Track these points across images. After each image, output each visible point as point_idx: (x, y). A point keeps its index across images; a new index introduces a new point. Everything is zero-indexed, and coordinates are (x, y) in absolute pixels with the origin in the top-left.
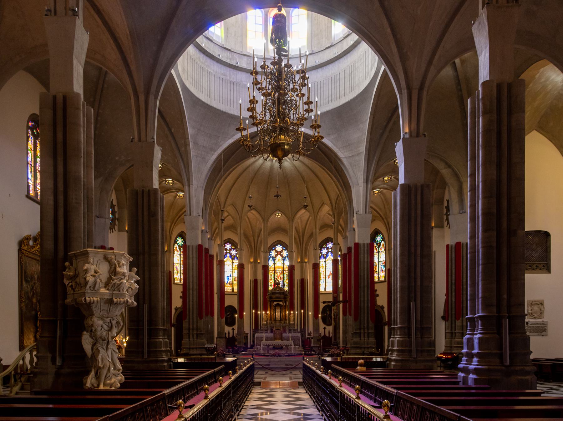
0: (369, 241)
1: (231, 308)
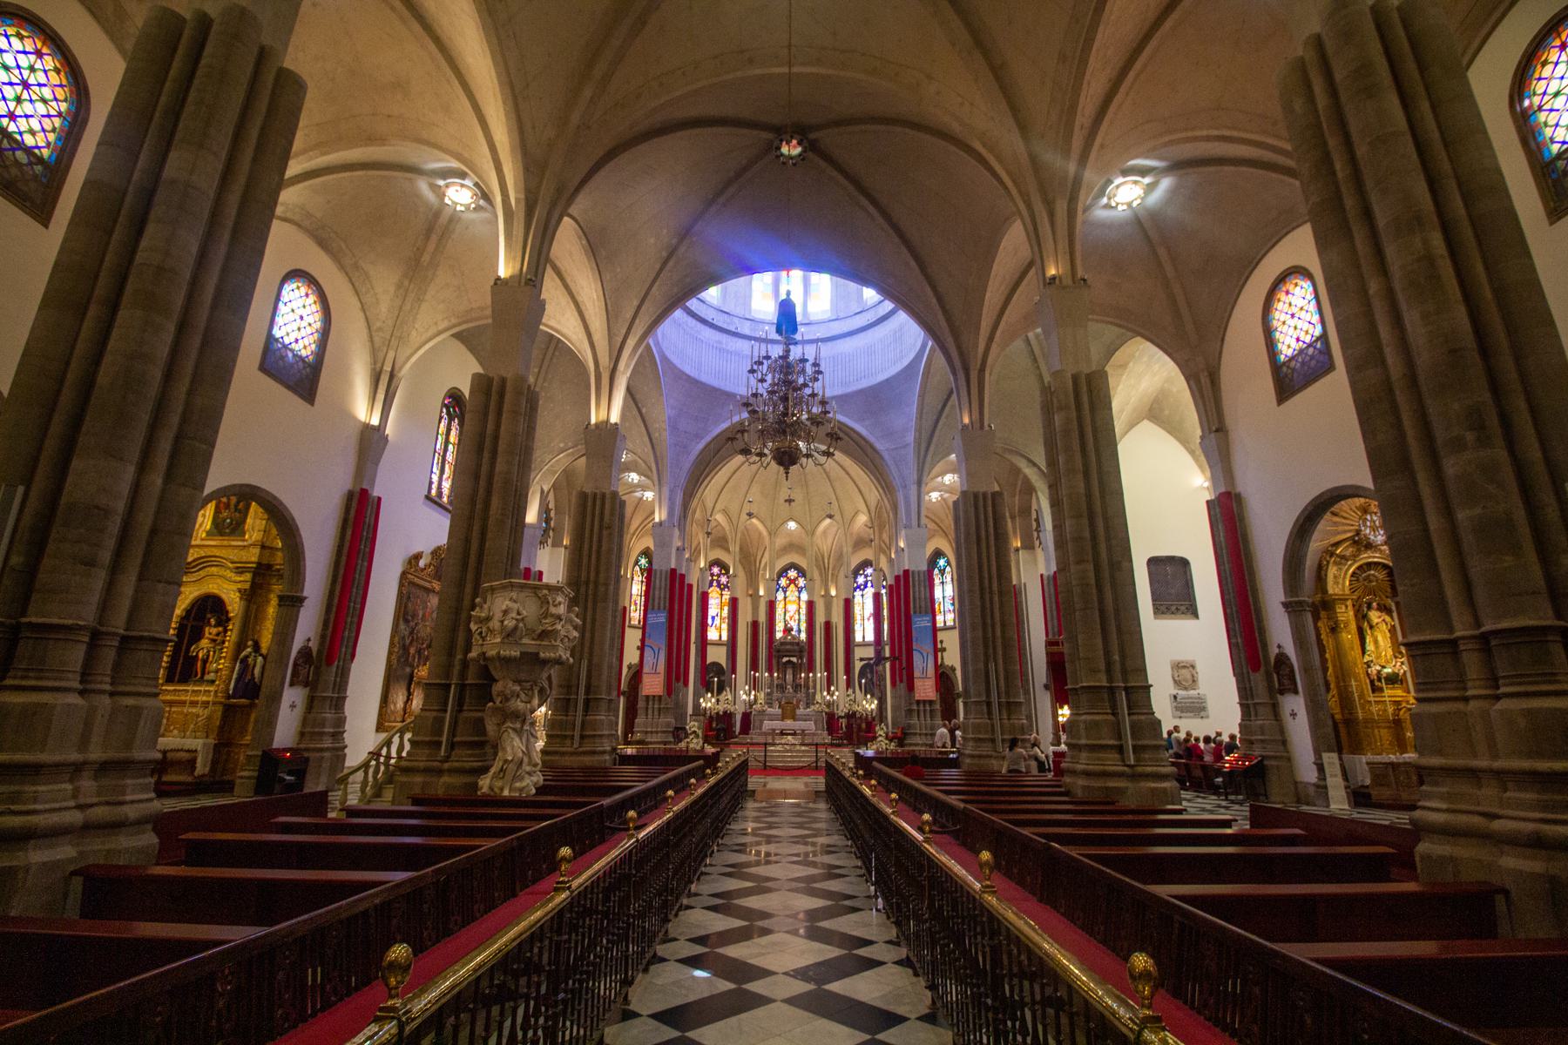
0: (925, 568)
1: (715, 664)
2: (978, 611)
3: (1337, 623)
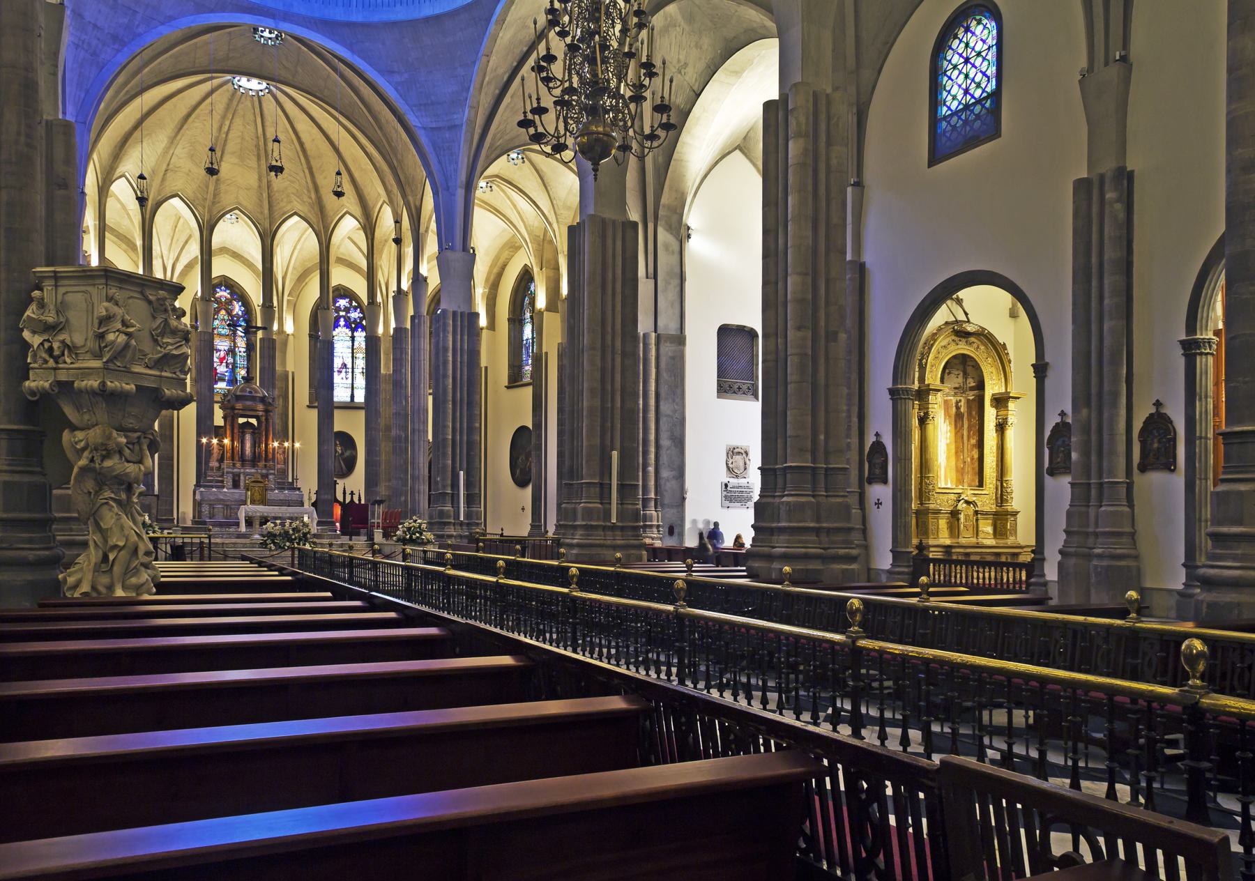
2: (598, 375)
3: (927, 414)
